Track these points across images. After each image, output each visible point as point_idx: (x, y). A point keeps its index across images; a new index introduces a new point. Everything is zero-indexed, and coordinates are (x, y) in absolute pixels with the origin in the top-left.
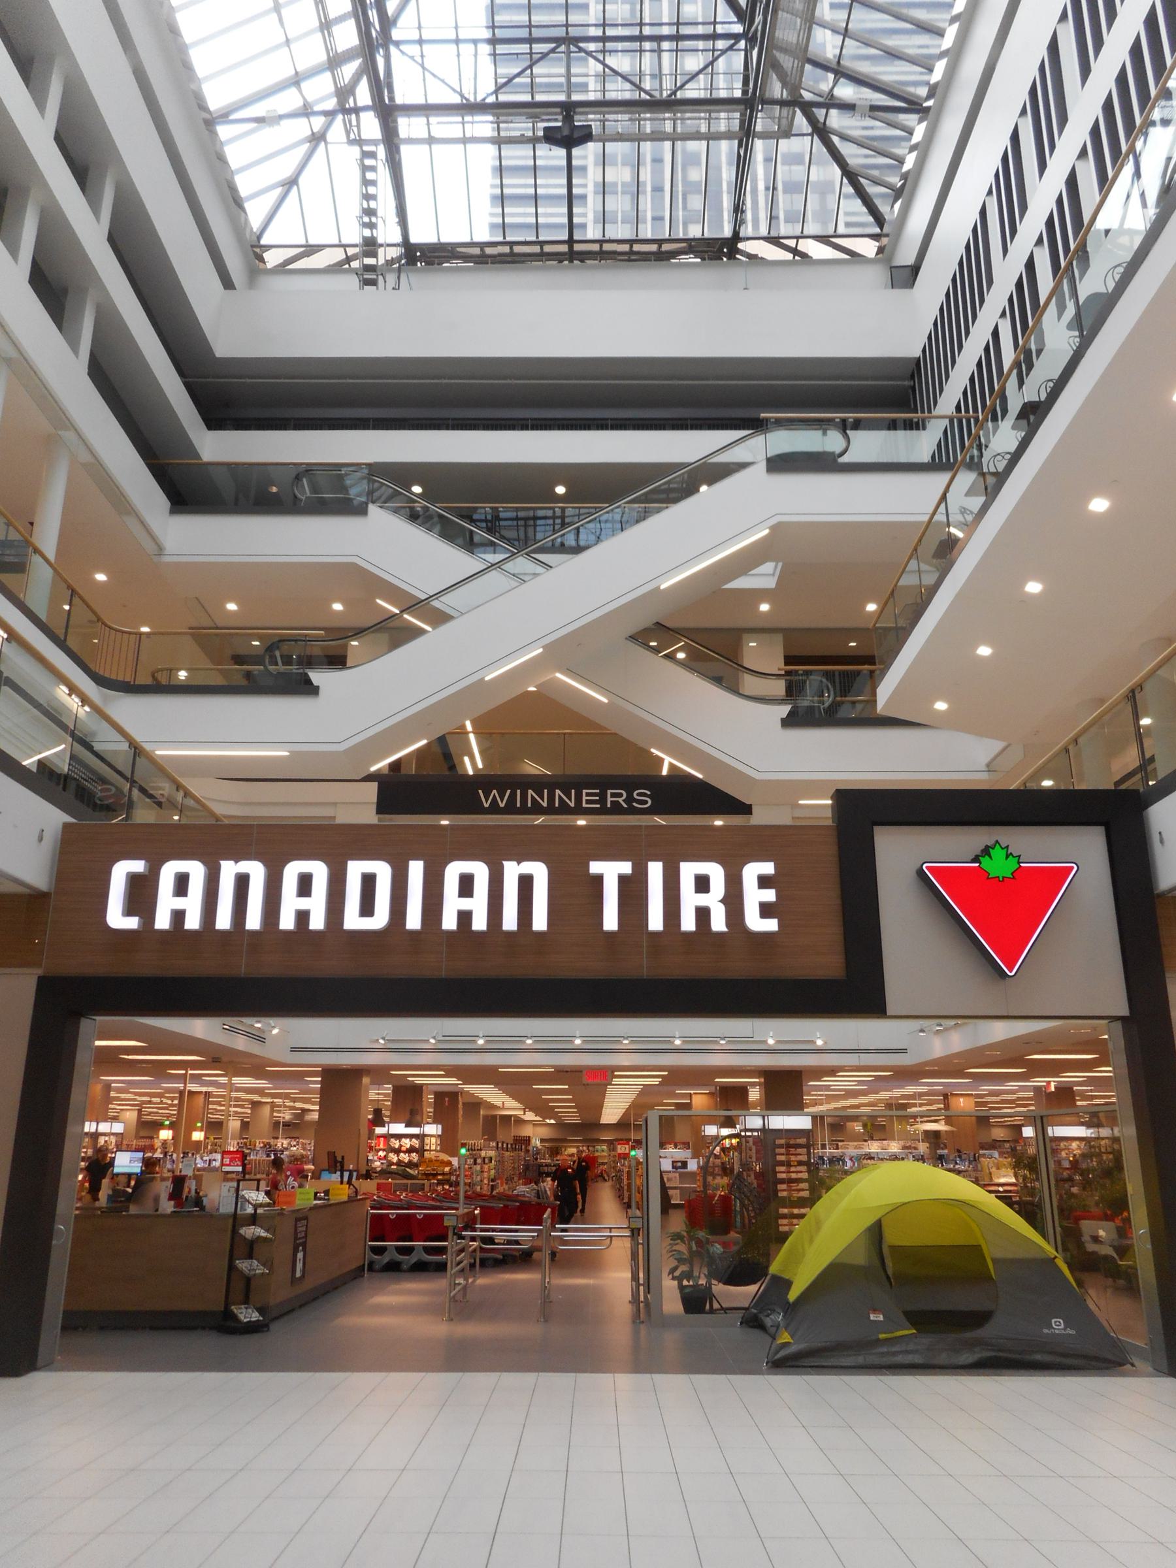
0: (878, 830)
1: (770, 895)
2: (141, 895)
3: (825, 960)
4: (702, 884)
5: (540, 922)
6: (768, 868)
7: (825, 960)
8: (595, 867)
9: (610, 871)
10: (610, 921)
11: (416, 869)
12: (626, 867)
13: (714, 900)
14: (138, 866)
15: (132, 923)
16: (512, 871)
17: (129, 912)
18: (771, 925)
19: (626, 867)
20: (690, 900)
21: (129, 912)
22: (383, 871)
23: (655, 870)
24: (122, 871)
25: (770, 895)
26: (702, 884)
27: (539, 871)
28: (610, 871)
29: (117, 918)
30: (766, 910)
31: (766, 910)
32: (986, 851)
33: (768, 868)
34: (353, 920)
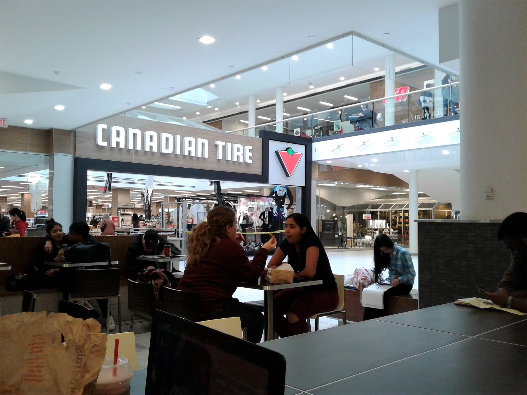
0: (270, 141)
1: (251, 154)
2: (107, 137)
3: (258, 171)
4: (238, 150)
5: (206, 156)
6: (251, 148)
7: (258, 171)
8: (218, 143)
9: (221, 144)
10: (220, 157)
11: (178, 137)
12: (224, 144)
13: (240, 154)
14: (105, 127)
15: (105, 144)
16: (200, 141)
17: (103, 140)
18: (251, 161)
19: (224, 144)
20: (236, 154)
21: (103, 140)
22: (170, 137)
23: (229, 145)
24: (101, 127)
25: (251, 154)
26: (238, 150)
27: (206, 142)
28: (221, 144)
29: (101, 142)
30: (250, 158)
31: (250, 158)
32: (287, 149)
33: (251, 148)
34: (164, 150)
